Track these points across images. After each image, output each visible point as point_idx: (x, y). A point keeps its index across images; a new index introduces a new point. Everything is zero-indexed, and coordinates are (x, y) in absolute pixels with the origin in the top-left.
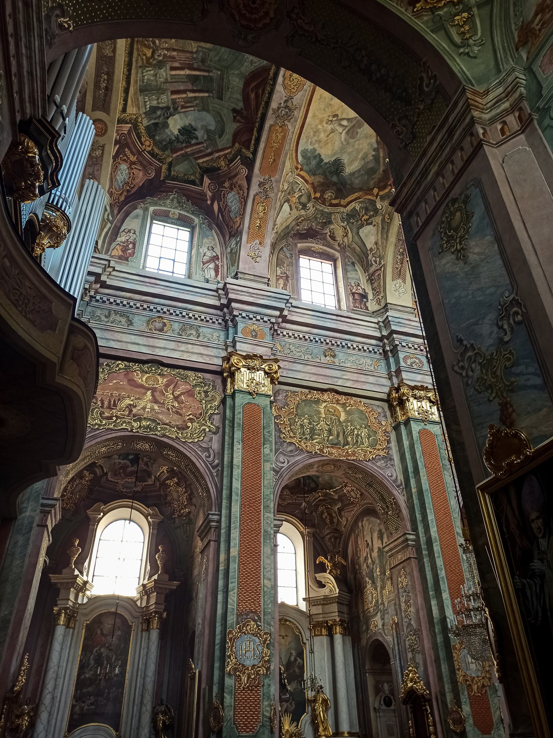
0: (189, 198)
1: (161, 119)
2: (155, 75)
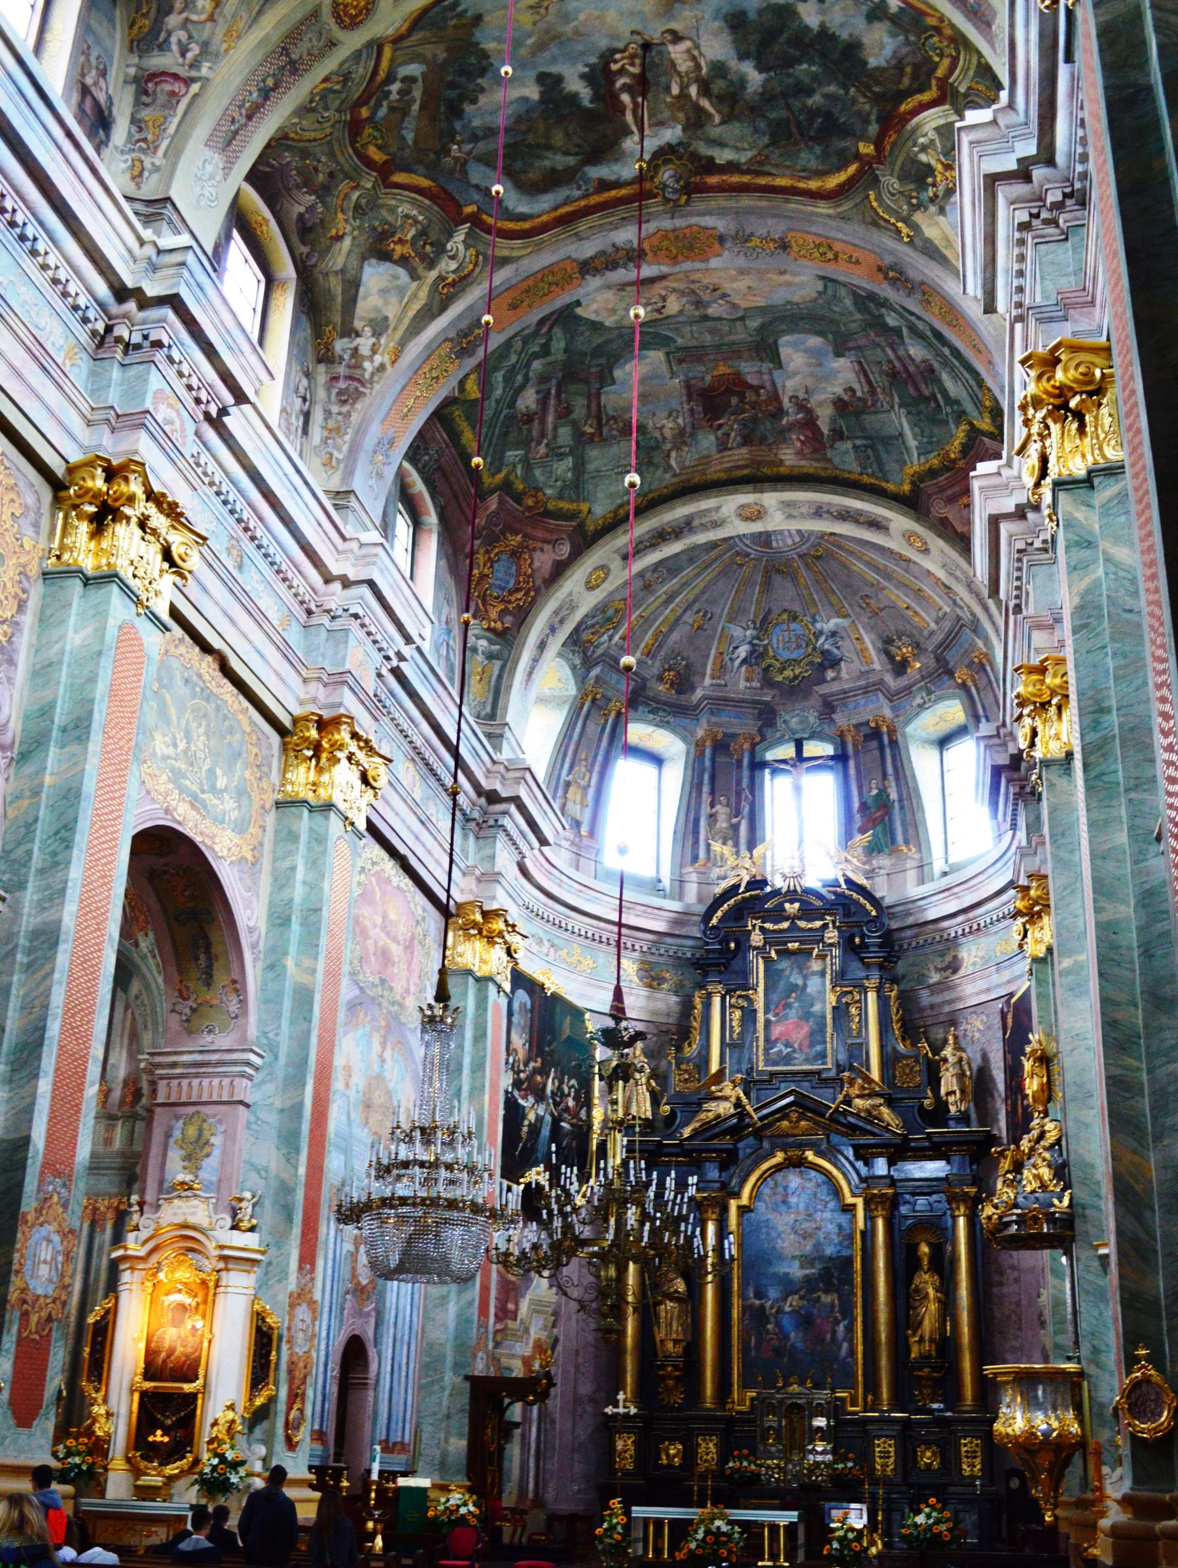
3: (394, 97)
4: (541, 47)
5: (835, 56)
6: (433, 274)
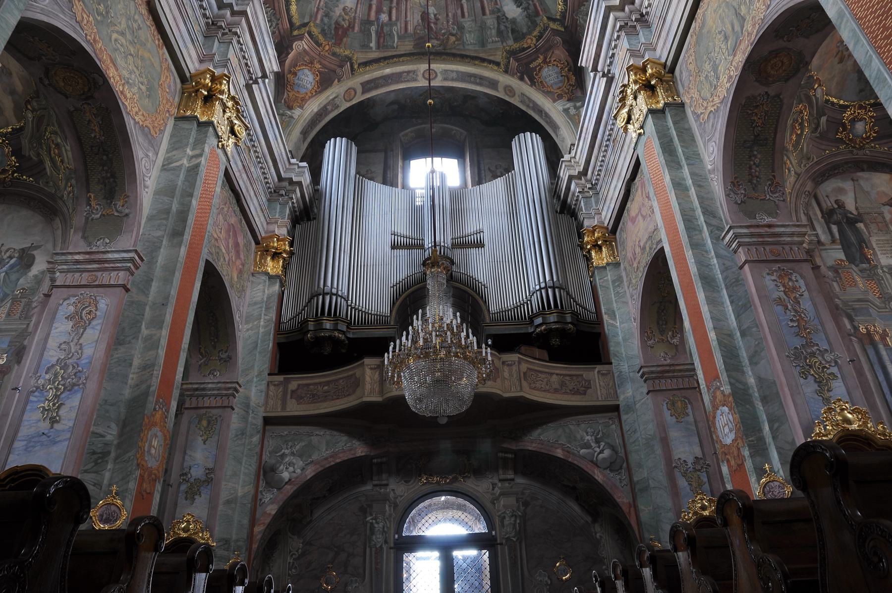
1: (508, 25)
2: (470, 32)
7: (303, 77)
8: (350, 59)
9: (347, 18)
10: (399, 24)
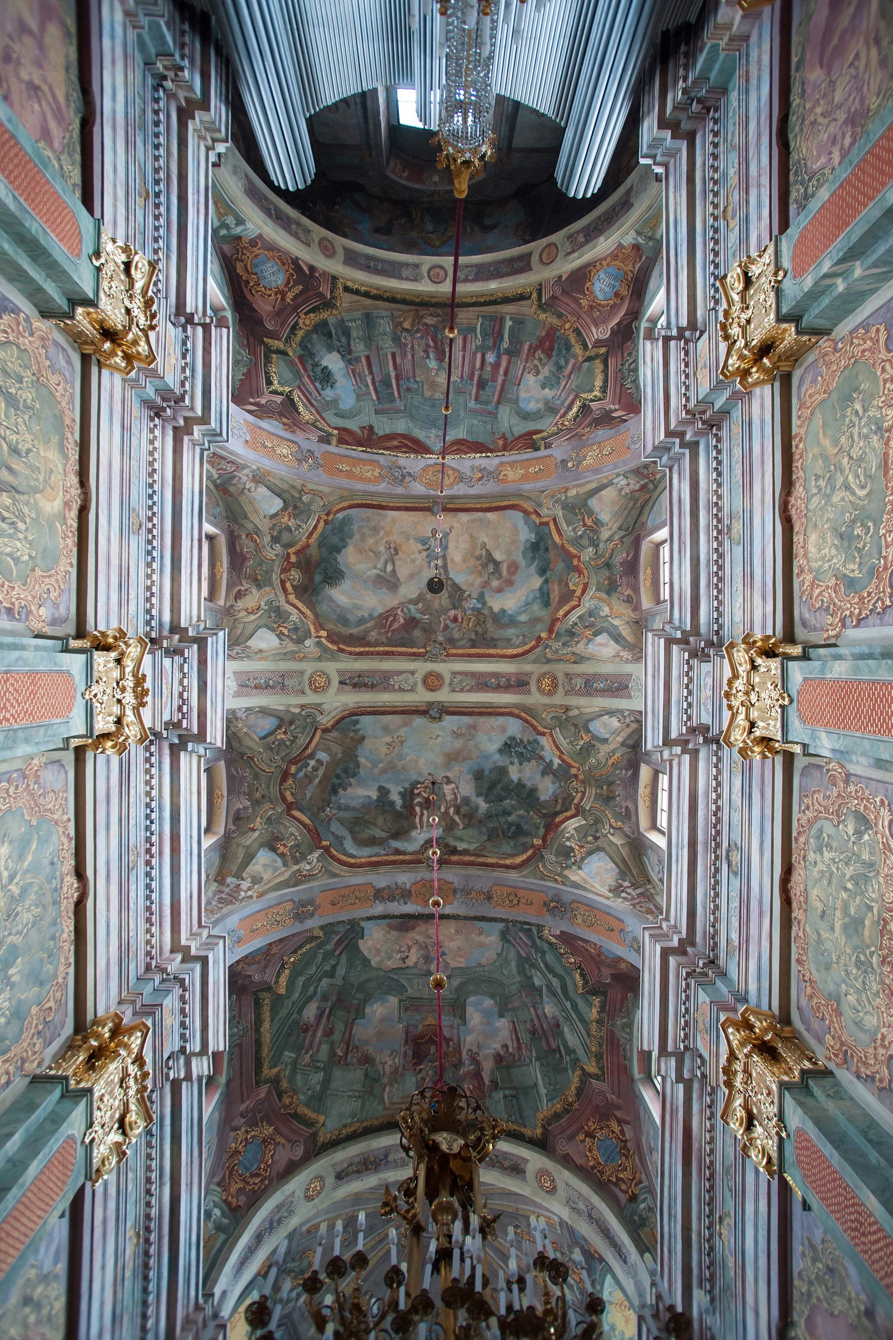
0: (248, 375)
2: (385, 334)
3: (309, 769)
4: (384, 771)
5: (524, 796)
6: (296, 867)
7: (607, 289)
8: (540, 306)
9: (536, 362)
10: (474, 347)
